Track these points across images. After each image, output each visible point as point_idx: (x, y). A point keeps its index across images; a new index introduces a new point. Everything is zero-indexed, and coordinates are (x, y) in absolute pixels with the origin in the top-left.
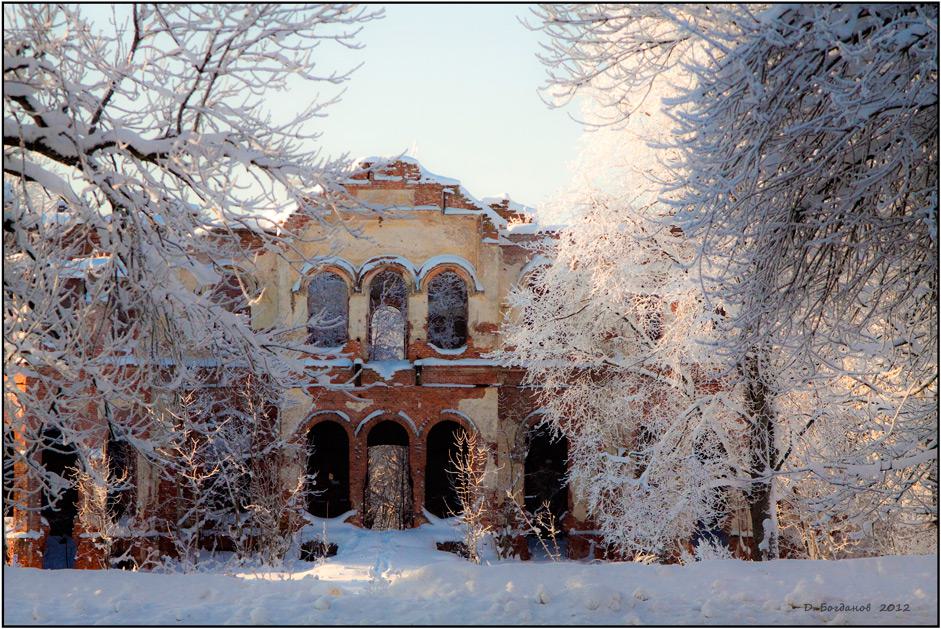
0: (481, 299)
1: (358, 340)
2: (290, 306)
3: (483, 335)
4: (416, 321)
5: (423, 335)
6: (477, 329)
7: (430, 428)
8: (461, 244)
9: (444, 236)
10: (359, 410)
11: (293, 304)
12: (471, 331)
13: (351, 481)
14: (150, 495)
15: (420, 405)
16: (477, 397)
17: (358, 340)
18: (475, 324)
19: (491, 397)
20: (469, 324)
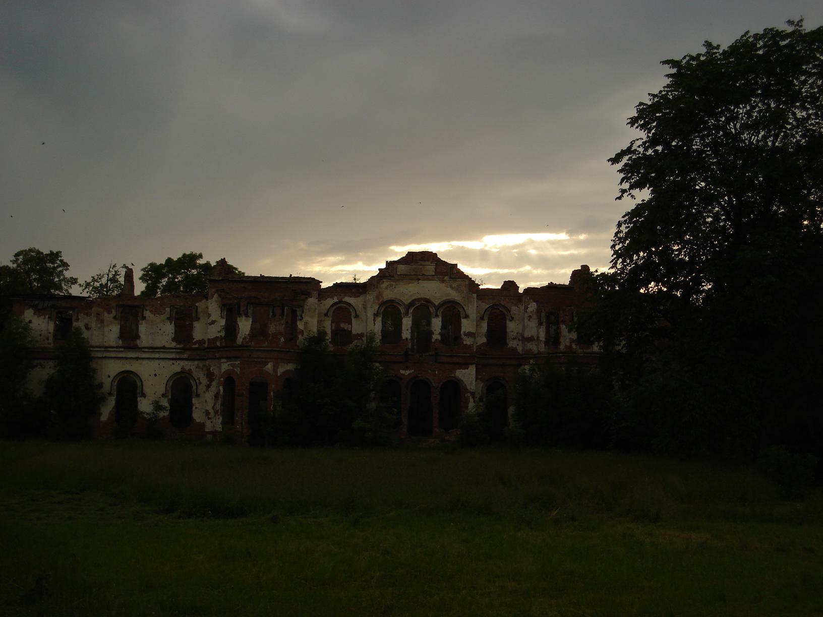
1: (407, 339)
4: (435, 330)
5: (439, 337)
10: (406, 374)
11: (374, 320)
12: (463, 336)
15: (437, 372)
17: (407, 339)
18: (464, 333)
19: (472, 370)
20: (462, 332)
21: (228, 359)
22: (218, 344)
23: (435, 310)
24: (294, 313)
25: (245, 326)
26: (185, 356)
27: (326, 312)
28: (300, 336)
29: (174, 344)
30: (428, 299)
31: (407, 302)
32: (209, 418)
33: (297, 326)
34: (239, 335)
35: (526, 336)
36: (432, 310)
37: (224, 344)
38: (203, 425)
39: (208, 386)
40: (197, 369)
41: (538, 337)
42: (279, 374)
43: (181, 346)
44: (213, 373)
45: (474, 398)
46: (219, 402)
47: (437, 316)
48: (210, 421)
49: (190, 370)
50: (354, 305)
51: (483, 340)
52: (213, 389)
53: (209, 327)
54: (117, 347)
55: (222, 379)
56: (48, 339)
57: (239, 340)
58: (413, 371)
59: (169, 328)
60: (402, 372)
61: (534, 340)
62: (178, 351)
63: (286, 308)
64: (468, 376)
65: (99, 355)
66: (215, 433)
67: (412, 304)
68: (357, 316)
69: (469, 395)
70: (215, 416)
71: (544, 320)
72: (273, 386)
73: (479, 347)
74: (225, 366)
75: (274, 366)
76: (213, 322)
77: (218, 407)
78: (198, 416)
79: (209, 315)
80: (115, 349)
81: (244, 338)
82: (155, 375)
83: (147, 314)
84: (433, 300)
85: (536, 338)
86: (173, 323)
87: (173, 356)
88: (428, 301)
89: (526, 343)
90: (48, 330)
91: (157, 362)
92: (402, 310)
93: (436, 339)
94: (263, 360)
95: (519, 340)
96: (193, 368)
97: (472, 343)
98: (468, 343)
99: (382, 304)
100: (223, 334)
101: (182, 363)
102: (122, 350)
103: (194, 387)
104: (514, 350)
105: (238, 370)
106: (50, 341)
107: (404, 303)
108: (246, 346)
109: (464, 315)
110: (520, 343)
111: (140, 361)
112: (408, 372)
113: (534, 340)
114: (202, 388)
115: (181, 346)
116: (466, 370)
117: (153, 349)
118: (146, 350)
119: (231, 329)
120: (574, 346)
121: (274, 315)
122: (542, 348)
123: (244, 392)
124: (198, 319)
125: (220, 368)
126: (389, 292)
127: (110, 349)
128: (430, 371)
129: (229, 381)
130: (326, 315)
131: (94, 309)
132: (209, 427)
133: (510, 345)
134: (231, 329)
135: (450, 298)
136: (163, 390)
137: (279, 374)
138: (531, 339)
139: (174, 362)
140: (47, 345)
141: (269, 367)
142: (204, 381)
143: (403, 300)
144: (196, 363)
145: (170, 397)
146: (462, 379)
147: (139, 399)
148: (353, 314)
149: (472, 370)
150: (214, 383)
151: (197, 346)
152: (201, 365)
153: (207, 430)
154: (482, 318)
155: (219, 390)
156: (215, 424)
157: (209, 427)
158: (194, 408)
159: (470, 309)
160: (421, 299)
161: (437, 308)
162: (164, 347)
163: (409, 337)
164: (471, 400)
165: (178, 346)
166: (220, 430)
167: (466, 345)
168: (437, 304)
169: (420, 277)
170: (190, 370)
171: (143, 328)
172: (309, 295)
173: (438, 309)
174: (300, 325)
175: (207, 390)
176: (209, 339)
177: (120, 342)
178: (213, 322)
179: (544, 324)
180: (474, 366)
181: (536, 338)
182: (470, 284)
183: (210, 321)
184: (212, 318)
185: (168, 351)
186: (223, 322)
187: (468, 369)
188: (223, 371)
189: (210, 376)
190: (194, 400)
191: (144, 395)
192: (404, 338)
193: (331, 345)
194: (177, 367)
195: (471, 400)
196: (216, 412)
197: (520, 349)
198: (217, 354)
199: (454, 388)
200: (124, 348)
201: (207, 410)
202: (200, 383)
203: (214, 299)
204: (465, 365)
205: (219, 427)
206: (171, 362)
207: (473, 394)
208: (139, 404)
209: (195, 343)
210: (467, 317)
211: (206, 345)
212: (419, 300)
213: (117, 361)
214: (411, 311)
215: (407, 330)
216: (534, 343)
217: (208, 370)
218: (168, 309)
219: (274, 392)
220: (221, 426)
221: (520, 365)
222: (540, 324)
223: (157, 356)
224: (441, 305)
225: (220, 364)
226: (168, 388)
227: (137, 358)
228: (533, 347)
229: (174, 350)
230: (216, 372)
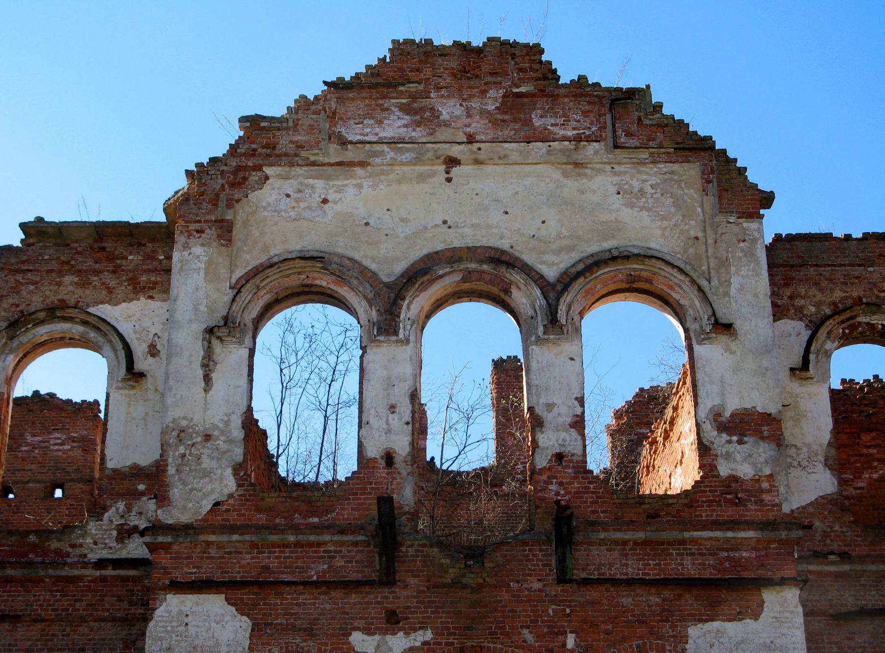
0: (728, 349)
2: (200, 373)
3: (740, 442)
8: (664, 218)
9: (617, 202)
11: (208, 364)
16: (737, 617)
23: (540, 301)
30: (503, 252)
50: (125, 328)
58: (429, 635)
84: (528, 258)
93: (559, 457)
97: (767, 471)
98: (745, 471)
107: (367, 276)
116: (749, 623)
135: (623, 243)
143: (366, 263)
159: (733, 291)
160: (472, 252)
167: (734, 479)
168: (551, 273)
169: (455, 151)
180: (791, 595)
187: (756, 616)
215: (392, 408)
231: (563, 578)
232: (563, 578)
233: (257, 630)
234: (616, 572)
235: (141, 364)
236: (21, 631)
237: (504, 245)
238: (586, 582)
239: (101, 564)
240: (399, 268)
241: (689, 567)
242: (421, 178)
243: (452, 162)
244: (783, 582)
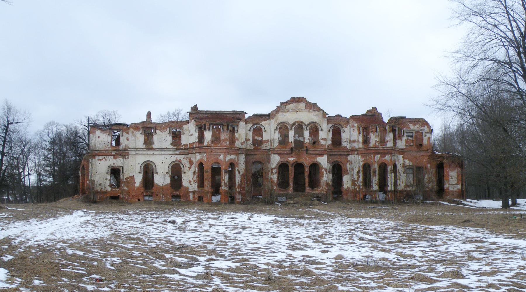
1: (292, 142)
5: (308, 141)
6: (321, 140)
7: (310, 164)
10: (292, 160)
11: (275, 132)
12: (320, 140)
13: (290, 178)
14: (239, 182)
17: (292, 142)
19: (325, 157)
20: (320, 138)
21: (200, 153)
22: (195, 146)
24: (234, 129)
25: (208, 135)
26: (178, 152)
27: (249, 129)
28: (237, 141)
29: (172, 147)
31: (291, 123)
32: (191, 184)
33: (235, 136)
34: (205, 141)
35: (352, 140)
36: (304, 127)
37: (197, 146)
38: (187, 188)
39: (190, 168)
40: (184, 159)
41: (358, 141)
42: (226, 161)
43: (175, 147)
44: (192, 161)
45: (326, 172)
46: (196, 175)
47: (307, 130)
48: (191, 185)
49: (180, 160)
51: (330, 142)
52: (193, 169)
53: (190, 137)
54: (143, 149)
55: (197, 164)
56: (108, 146)
57: (205, 144)
59: (169, 138)
60: (289, 159)
61: (356, 142)
62: (174, 150)
63: (229, 126)
64: (323, 161)
65: (133, 153)
66: (194, 192)
67: (294, 124)
68: (265, 131)
69: (324, 170)
70: (194, 183)
71: (361, 131)
72: (224, 167)
73: (328, 146)
74: (198, 157)
75: (224, 156)
76: (192, 135)
77: (195, 178)
78: (185, 183)
79: (190, 131)
80: (141, 150)
81: (208, 142)
82: (163, 163)
83: (157, 131)
85: (357, 141)
86: (171, 135)
87: (171, 153)
88: (302, 122)
89: (352, 143)
90: (108, 141)
91: (163, 156)
92: (289, 128)
94: (218, 153)
95: (348, 142)
96: (182, 159)
98: (323, 144)
99: (279, 124)
100: (197, 141)
101: (176, 156)
102: (145, 150)
103: (183, 169)
104: (345, 147)
105: (205, 159)
106: (109, 147)
107: (290, 124)
108: (209, 146)
109: (321, 129)
110: (348, 144)
111: (154, 156)
112: (292, 159)
113: (356, 142)
114: (187, 169)
115: (175, 147)
117: (161, 149)
118: (158, 150)
119: (201, 138)
120: (377, 144)
121: (223, 130)
122: (361, 146)
123: (209, 170)
124: (184, 133)
125: (196, 158)
126: (282, 117)
127: (139, 150)
128: (304, 158)
129: (201, 165)
130: (250, 130)
131: (131, 130)
132: (191, 189)
133: (343, 145)
134: (201, 138)
136: (167, 171)
137: (226, 161)
138: (354, 141)
139: (172, 156)
140: (108, 149)
141: (221, 157)
142: (188, 165)
144: (183, 156)
145: (170, 174)
146: (320, 162)
147: (154, 175)
148: (263, 130)
149: (325, 157)
150: (193, 166)
151: (184, 147)
152: (186, 157)
153: (189, 190)
154: (329, 131)
155: (196, 170)
156: (194, 187)
157: (191, 189)
158: (183, 179)
161: (307, 126)
162: (167, 148)
163: (293, 141)
164: (325, 173)
165: (174, 148)
166: (197, 190)
168: (306, 124)
169: (298, 110)
170: (180, 160)
171: (155, 137)
172: (241, 120)
173: (308, 126)
174: (237, 135)
175: (189, 170)
176: (189, 144)
177: (144, 146)
178: (192, 135)
179: (362, 133)
181: (357, 141)
182: (324, 114)
183: (190, 134)
184: (191, 133)
185: (169, 150)
186: (196, 134)
188: (197, 160)
189: (191, 163)
190: (183, 175)
191: (157, 173)
192: (290, 141)
193: (252, 146)
194: (174, 158)
195: (325, 173)
196: (195, 181)
197: (348, 147)
198: (194, 151)
199: (315, 167)
200: (147, 149)
201: (189, 180)
202: (186, 167)
203: (192, 123)
204: (321, 155)
205: (196, 189)
206: (171, 156)
207: (326, 170)
208: (154, 178)
209: (182, 146)
210: (322, 130)
211: (188, 147)
212: (297, 122)
213: (143, 156)
214: (293, 127)
216: (356, 143)
217: (190, 159)
218: (168, 129)
219: (224, 170)
220: (197, 188)
221: (349, 155)
222: (360, 133)
223: (163, 153)
224: (308, 125)
225: (196, 156)
226: (169, 169)
227: (153, 154)
228: (355, 146)
229: (172, 150)
230: (194, 160)
231: (307, 153)
232: (307, 153)
233: (281, 158)
234: (311, 153)
235: (266, 129)
236: (257, 156)
237: (302, 120)
238: (309, 154)
239: (264, 149)
240: (292, 123)
241: (318, 152)
242: (294, 113)
243: (297, 111)
244: (325, 154)
